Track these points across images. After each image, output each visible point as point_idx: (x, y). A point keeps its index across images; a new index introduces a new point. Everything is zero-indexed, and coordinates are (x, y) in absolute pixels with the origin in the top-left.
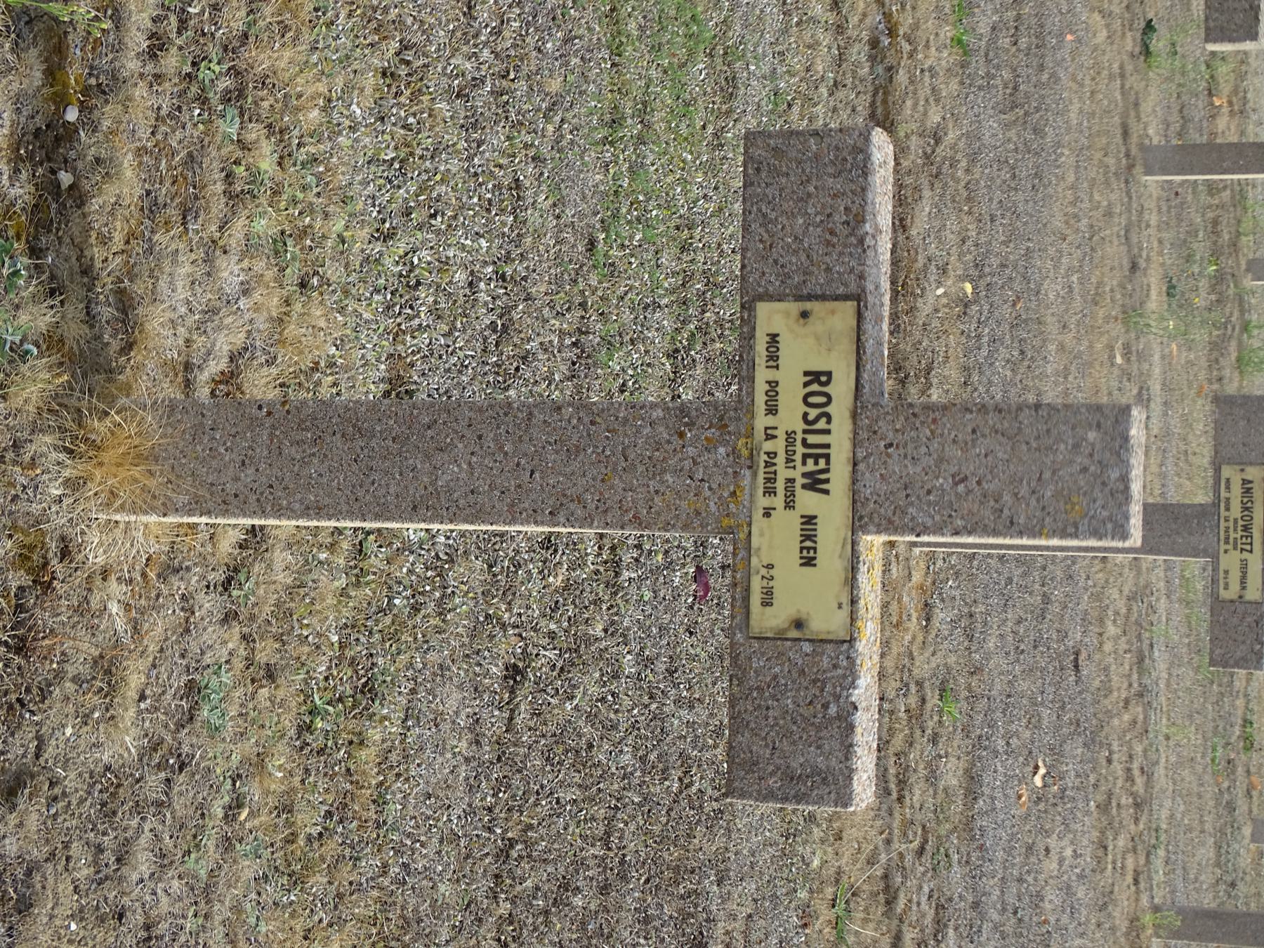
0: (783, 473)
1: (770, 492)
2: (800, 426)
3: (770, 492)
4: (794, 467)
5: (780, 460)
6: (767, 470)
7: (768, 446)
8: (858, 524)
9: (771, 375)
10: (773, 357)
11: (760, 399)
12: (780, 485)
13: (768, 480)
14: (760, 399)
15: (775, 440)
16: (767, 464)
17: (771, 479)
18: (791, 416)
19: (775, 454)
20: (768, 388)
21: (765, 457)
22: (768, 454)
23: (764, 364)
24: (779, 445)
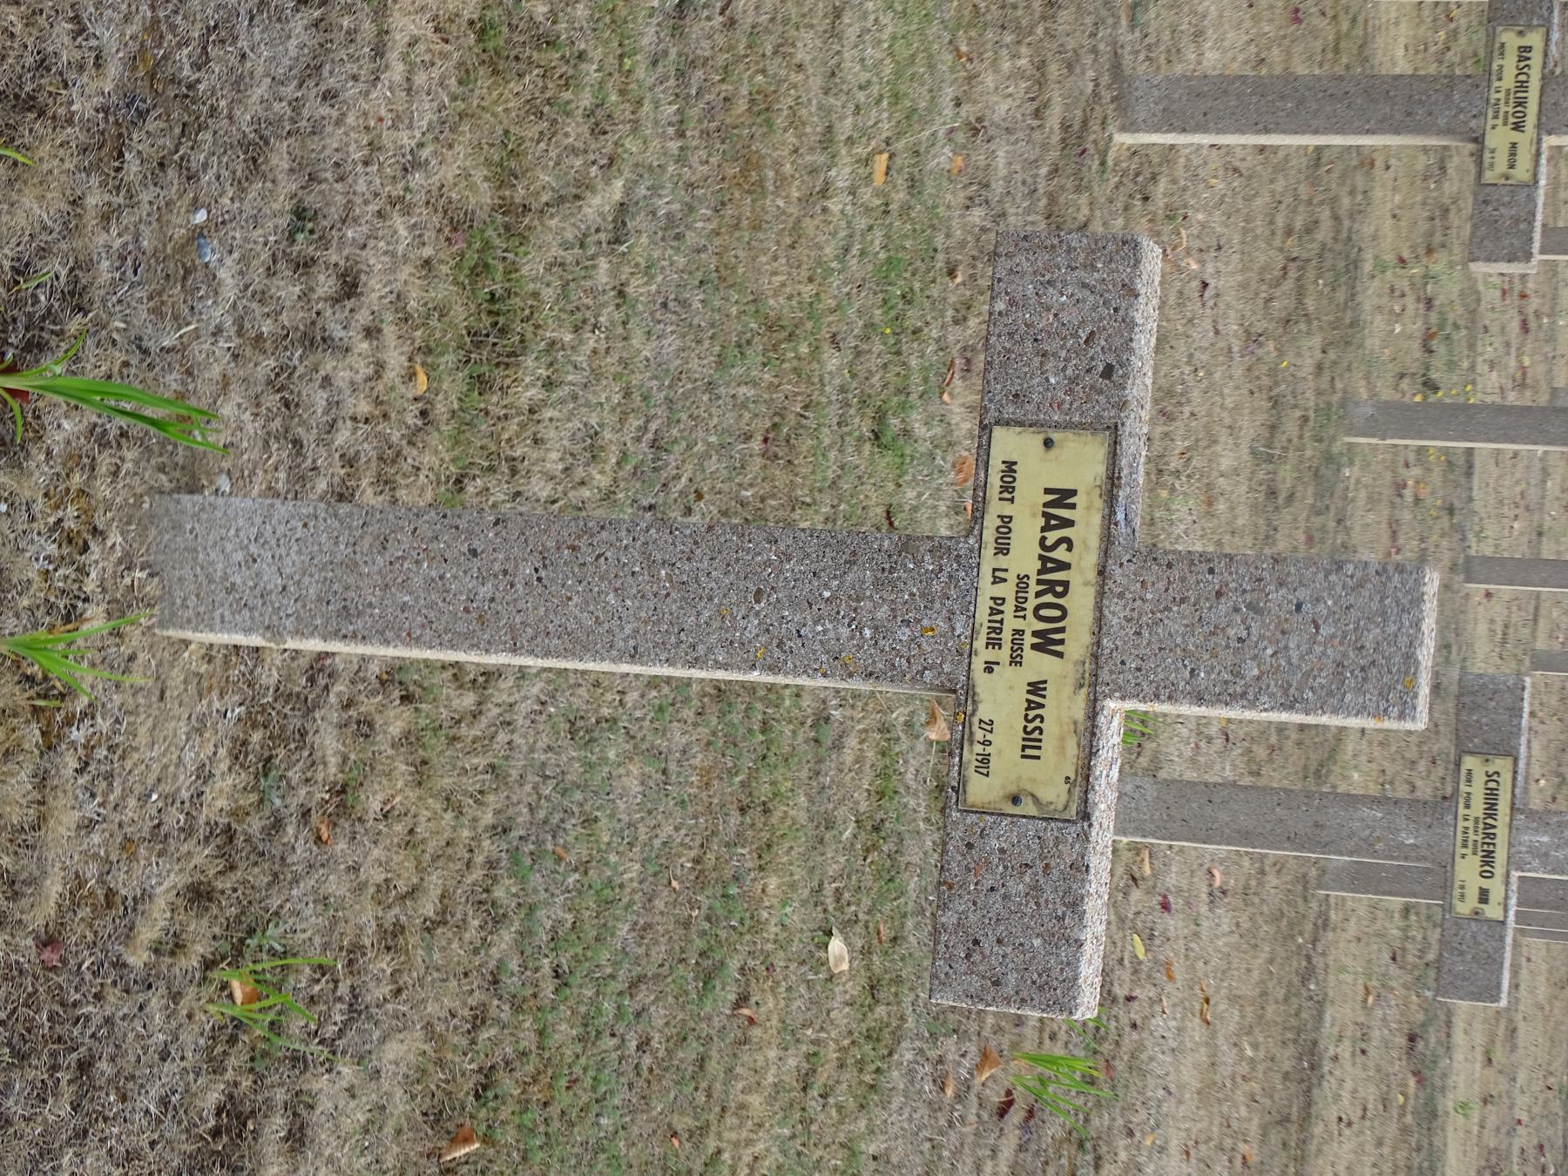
0: (1011, 623)
1: (994, 643)
2: (1032, 566)
3: (994, 643)
4: (1024, 617)
5: (1009, 608)
6: (998, 617)
7: (999, 590)
8: (1094, 687)
9: (1007, 509)
10: (1008, 488)
11: (989, 535)
12: (1007, 636)
13: (993, 630)
14: (989, 535)
15: (1002, 585)
16: (993, 611)
17: (996, 630)
20: (999, 523)
21: (991, 603)
23: (997, 496)
24: (1007, 590)
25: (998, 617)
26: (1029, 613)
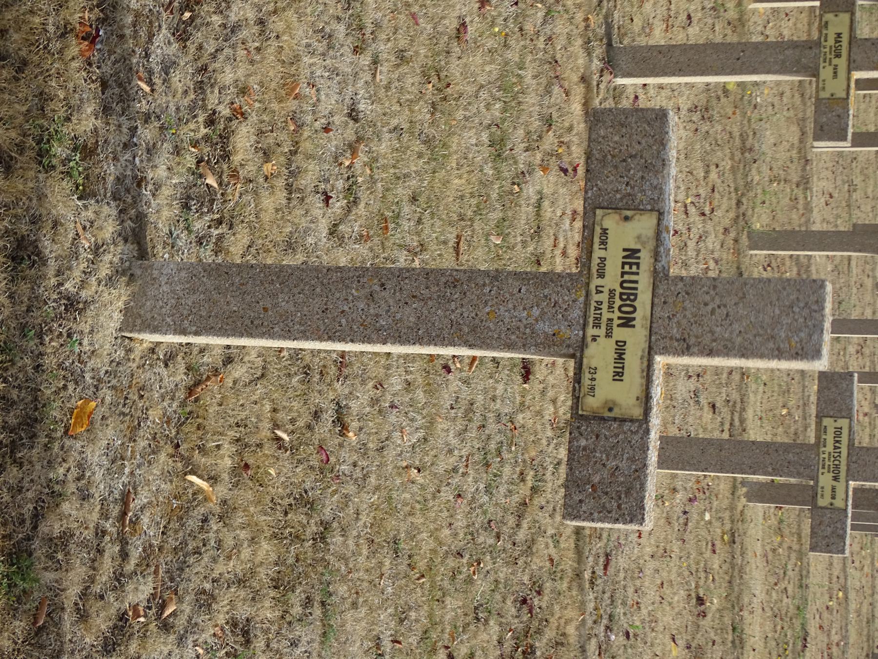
0: (606, 315)
1: (597, 325)
3: (597, 325)
5: (605, 306)
13: (596, 319)
14: (594, 268)
16: (596, 309)
18: (612, 280)
19: (602, 302)
21: (595, 304)
22: (597, 302)
24: (604, 297)
25: (599, 312)
26: (616, 310)
